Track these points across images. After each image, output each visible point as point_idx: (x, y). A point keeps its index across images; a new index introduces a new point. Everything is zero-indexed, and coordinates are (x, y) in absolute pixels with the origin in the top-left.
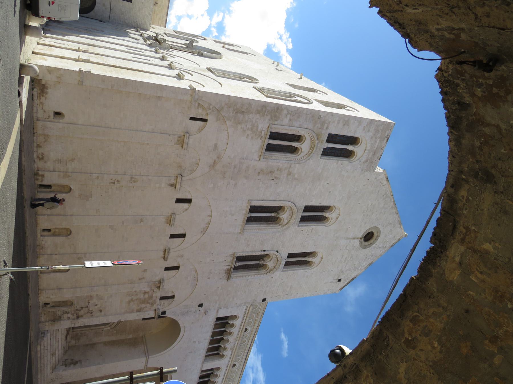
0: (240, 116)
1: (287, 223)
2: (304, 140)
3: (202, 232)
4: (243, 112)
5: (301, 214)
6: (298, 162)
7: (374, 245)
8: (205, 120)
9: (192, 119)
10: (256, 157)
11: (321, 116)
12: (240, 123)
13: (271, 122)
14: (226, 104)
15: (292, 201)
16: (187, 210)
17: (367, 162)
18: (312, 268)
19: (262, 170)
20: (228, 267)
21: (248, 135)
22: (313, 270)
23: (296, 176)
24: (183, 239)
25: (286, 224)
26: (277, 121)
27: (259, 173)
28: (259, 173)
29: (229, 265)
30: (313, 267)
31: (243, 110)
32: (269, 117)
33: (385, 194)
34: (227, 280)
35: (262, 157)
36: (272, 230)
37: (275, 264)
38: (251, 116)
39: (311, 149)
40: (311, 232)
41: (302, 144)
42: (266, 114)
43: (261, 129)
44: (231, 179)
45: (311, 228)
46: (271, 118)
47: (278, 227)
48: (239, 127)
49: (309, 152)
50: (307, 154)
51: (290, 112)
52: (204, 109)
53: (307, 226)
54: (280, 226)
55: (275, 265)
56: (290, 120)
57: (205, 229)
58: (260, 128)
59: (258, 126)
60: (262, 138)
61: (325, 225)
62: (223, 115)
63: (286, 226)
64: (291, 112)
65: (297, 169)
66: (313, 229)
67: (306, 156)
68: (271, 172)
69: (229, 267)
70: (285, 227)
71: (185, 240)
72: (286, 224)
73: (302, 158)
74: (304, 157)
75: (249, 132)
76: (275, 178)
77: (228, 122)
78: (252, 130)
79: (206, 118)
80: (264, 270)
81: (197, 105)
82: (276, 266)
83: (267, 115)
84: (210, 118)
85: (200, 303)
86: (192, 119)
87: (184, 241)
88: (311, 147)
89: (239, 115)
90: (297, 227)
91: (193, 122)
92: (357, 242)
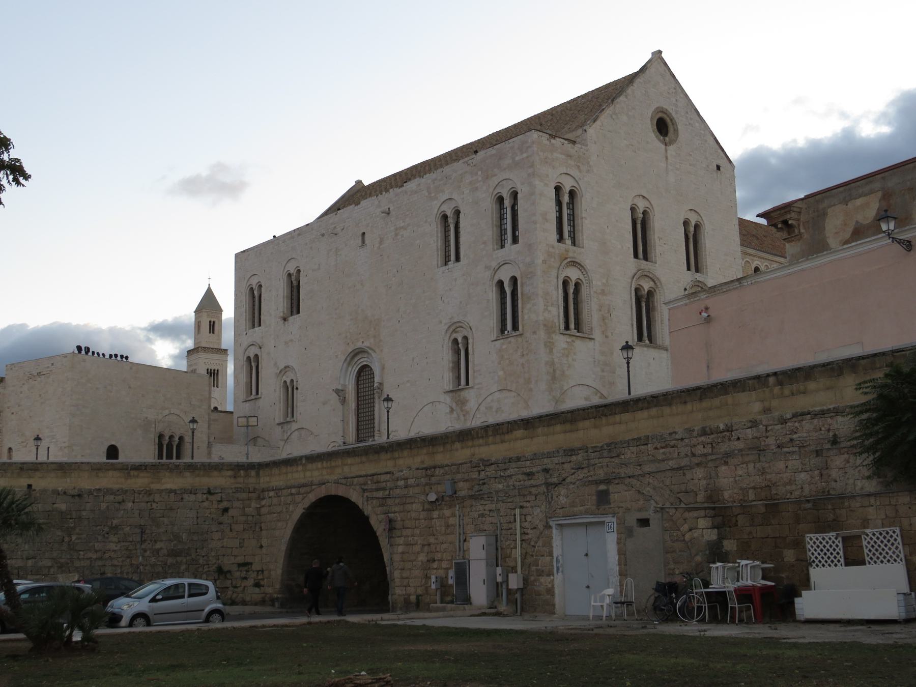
0: (558, 372)
1: (653, 281)
2: (566, 278)
4: (554, 371)
6: (590, 282)
7: (674, 114)
10: (590, 344)
11: (543, 260)
12: (563, 372)
13: (558, 331)
15: (630, 281)
17: (579, 166)
18: (702, 224)
19: (603, 332)
21: (573, 360)
22: (705, 221)
23: (604, 281)
25: (655, 283)
26: (555, 324)
27: (607, 337)
30: (701, 222)
32: (553, 335)
33: (612, 117)
38: (556, 360)
39: (575, 266)
40: (662, 239)
41: (571, 280)
42: (551, 341)
43: (565, 343)
44: (615, 373)
45: (657, 241)
46: (554, 332)
47: (658, 293)
50: (581, 270)
51: (546, 307)
53: (655, 246)
54: (657, 291)
56: (552, 305)
58: (565, 346)
59: (564, 349)
60: (573, 341)
62: (559, 395)
63: (656, 282)
64: (545, 306)
65: (597, 282)
66: (658, 237)
67: (582, 271)
68: (603, 320)
70: (658, 284)
72: (655, 283)
73: (585, 276)
74: (584, 273)
76: (609, 311)
77: (565, 388)
78: (567, 356)
83: (552, 339)
88: (573, 265)
90: (657, 265)
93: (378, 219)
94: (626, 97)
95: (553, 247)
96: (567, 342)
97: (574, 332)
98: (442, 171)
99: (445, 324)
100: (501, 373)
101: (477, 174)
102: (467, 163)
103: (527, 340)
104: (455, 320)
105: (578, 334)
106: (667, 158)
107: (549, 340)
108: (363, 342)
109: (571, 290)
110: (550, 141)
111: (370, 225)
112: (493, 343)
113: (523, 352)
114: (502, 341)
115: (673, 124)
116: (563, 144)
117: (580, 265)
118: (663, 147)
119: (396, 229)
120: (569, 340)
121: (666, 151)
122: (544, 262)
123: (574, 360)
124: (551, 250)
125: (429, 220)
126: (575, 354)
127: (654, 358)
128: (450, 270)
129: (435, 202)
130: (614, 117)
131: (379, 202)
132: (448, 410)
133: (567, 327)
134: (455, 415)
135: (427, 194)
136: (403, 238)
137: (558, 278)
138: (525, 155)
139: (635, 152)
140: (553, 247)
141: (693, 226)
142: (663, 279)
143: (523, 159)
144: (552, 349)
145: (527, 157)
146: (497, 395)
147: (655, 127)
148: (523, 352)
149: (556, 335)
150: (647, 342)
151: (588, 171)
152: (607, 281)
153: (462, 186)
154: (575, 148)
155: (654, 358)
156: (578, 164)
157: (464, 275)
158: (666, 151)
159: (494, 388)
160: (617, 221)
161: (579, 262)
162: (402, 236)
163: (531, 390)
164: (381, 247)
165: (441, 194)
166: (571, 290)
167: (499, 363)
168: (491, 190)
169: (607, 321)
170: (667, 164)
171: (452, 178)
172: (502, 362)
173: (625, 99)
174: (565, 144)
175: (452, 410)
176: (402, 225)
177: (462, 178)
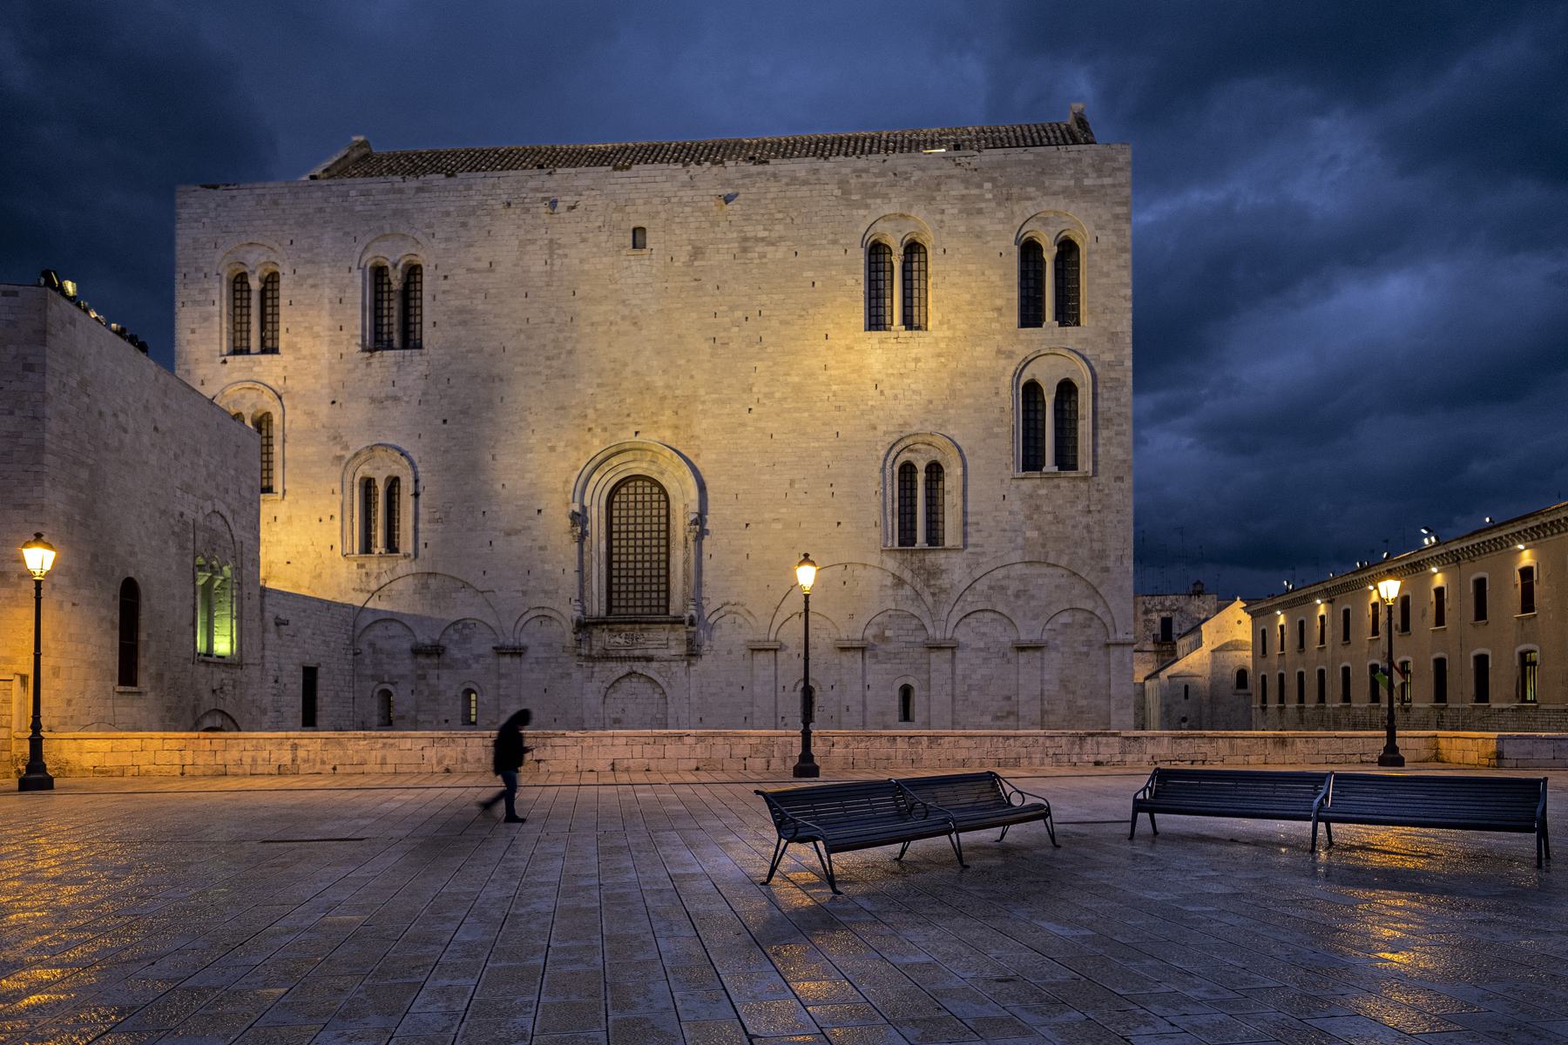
93: (688, 209)
98: (885, 161)
99: (885, 433)
100: (1033, 534)
101: (980, 186)
102: (954, 160)
103: (1100, 487)
104: (915, 429)
108: (637, 433)
111: (663, 216)
112: (1014, 482)
113: (1088, 506)
114: (1038, 482)
128: (899, 340)
129: (862, 212)
131: (691, 178)
132: (889, 581)
134: (907, 590)
135: (838, 192)
136: (764, 260)
138: (1107, 181)
143: (1103, 186)
145: (1114, 186)
146: (1019, 570)
148: (1088, 506)
153: (938, 198)
157: (939, 355)
159: (1016, 556)
162: (763, 256)
163: (1106, 570)
164: (696, 263)
165: (879, 201)
167: (1030, 518)
168: (1018, 222)
171: (913, 179)
172: (1035, 516)
175: (899, 582)
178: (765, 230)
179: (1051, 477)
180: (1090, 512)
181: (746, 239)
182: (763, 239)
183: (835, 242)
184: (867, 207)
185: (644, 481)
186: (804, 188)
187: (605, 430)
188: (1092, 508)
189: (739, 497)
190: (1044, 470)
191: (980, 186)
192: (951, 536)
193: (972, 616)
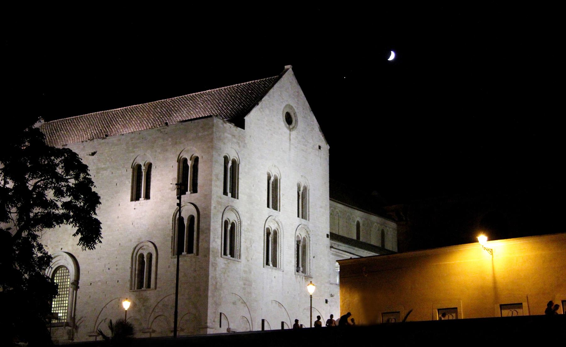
3: (281, 308)
4: (216, 283)
5: (271, 209)
8: (221, 313)
9: (220, 327)
12: (221, 284)
14: (213, 299)
16: (268, 323)
20: (304, 279)
22: (310, 184)
23: (249, 222)
24: (284, 323)
25: (278, 225)
28: (248, 261)
29: (302, 278)
31: (215, 284)
33: (260, 110)
34: (312, 278)
35: (239, 260)
36: (282, 239)
37: (303, 230)
41: (229, 221)
43: (224, 264)
48: (223, 285)
49: (235, 212)
52: (215, 317)
55: (304, 229)
57: (279, 304)
58: (223, 266)
59: (223, 268)
61: (280, 180)
63: (279, 225)
68: (247, 249)
69: (304, 277)
71: (285, 322)
72: (278, 225)
75: (226, 275)
78: (224, 273)
79: (219, 314)
80: (306, 239)
81: (214, 323)
82: (305, 228)
84: (220, 312)
85: (325, 302)
86: (220, 327)
87: (286, 323)
89: (218, 286)
91: (222, 324)
92: (294, 133)
94: (269, 97)
95: (221, 198)
96: (225, 263)
97: (229, 256)
102: (160, 131)
103: (199, 260)
105: (232, 258)
106: (290, 140)
107: (214, 262)
109: (229, 228)
110: (223, 125)
115: (295, 116)
116: (231, 128)
117: (237, 212)
118: (288, 131)
119: (98, 169)
120: (226, 262)
121: (290, 135)
122: (215, 208)
123: (228, 276)
124: (219, 200)
125: (126, 166)
126: (229, 272)
127: (275, 277)
129: (132, 154)
130: (261, 110)
131: (84, 146)
133: (225, 254)
135: (125, 147)
137: (222, 219)
138: (206, 133)
139: (272, 135)
140: (221, 198)
141: (303, 186)
142: (283, 223)
144: (216, 268)
145: (208, 135)
147: (285, 118)
149: (219, 258)
150: (271, 265)
151: (244, 147)
152: (251, 222)
154: (238, 130)
155: (275, 277)
156: (238, 141)
158: (290, 135)
160: (259, 182)
161: (235, 209)
166: (229, 228)
169: (248, 250)
170: (290, 144)
173: (268, 98)
174: (232, 128)
176: (103, 166)
177: (155, 141)
178: (104, 164)
179: (185, 256)
180: (195, 271)
181: (98, 169)
182: (103, 168)
183: (123, 167)
184: (134, 152)
185: (62, 268)
186: (116, 147)
187: (52, 248)
188: (196, 269)
189: (89, 272)
190: (183, 253)
191: (167, 140)
192: (152, 285)
193: (158, 318)
